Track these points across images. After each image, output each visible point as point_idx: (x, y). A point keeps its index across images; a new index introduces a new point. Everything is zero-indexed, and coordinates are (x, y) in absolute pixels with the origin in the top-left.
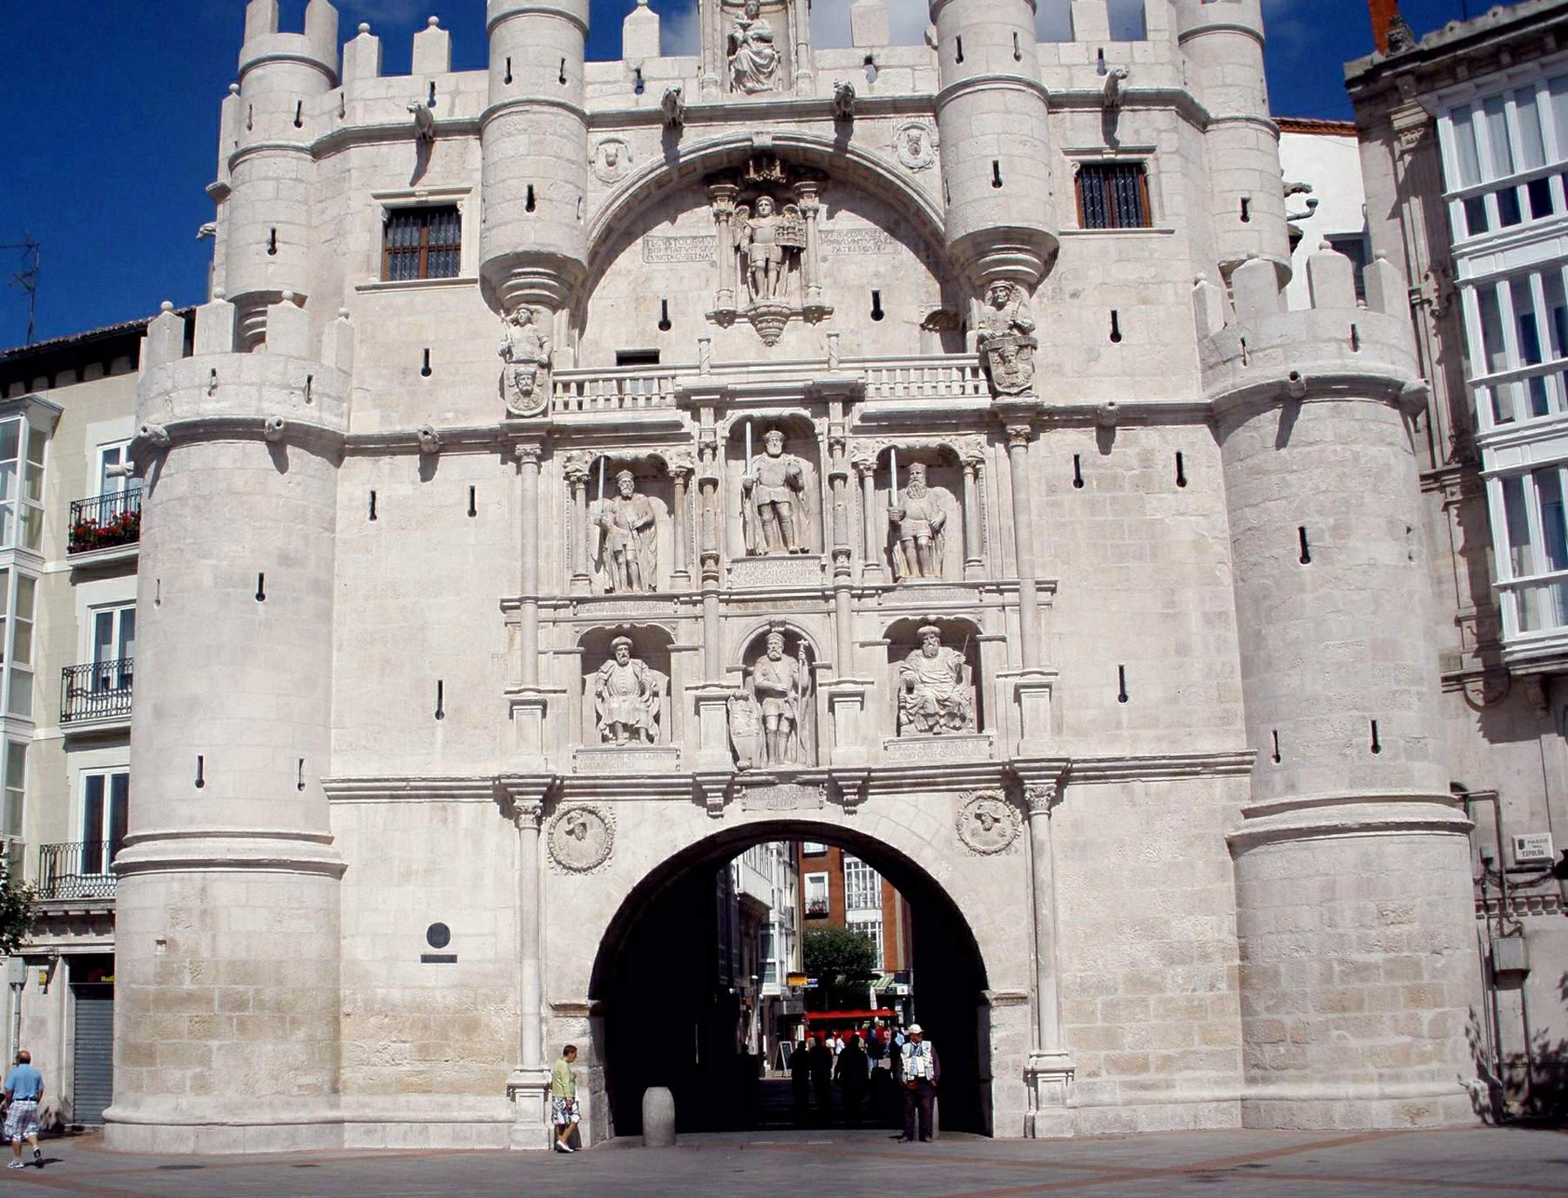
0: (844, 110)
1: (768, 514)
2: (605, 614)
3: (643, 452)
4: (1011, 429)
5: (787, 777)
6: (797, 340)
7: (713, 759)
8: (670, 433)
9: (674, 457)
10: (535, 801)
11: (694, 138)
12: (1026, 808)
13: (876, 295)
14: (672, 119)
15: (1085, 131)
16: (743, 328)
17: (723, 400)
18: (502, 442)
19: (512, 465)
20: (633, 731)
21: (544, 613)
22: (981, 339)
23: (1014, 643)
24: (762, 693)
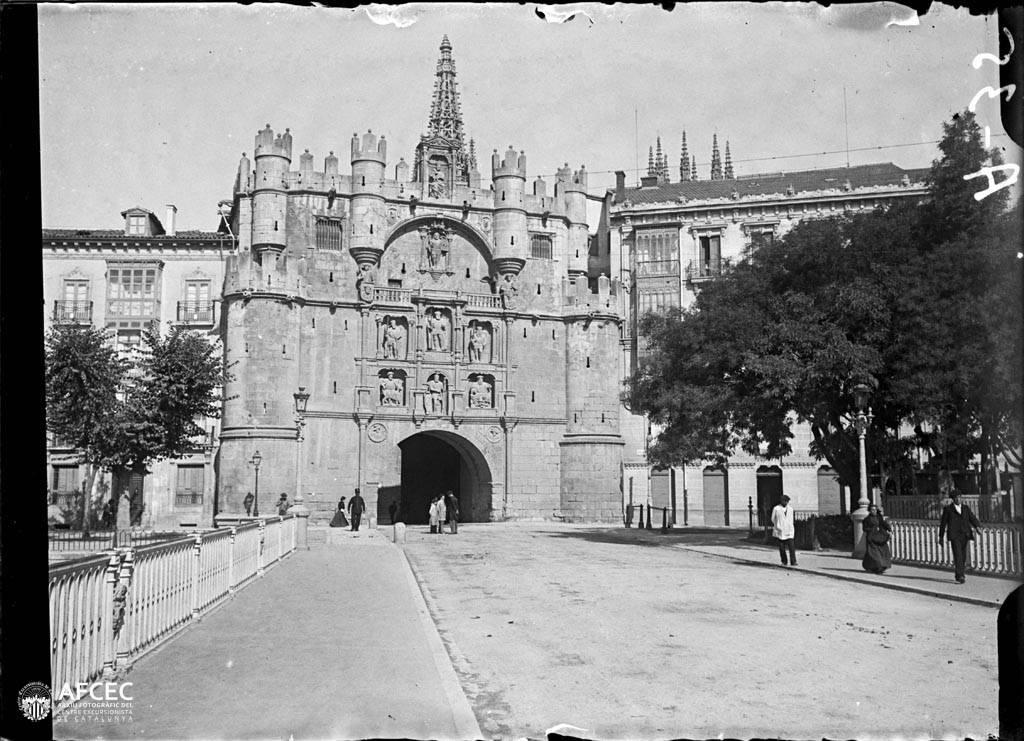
0: (466, 209)
1: (436, 338)
2: (386, 365)
3: (400, 315)
4: (508, 319)
5: (439, 418)
6: (446, 282)
7: (419, 412)
8: (410, 310)
9: (409, 317)
10: (365, 421)
11: (421, 212)
12: (506, 430)
13: (468, 270)
14: (413, 204)
15: (536, 225)
16: (427, 275)
17: (426, 301)
18: (358, 307)
19: (359, 313)
20: (394, 401)
21: (369, 363)
22: (501, 291)
23: (504, 382)
24: (432, 392)
